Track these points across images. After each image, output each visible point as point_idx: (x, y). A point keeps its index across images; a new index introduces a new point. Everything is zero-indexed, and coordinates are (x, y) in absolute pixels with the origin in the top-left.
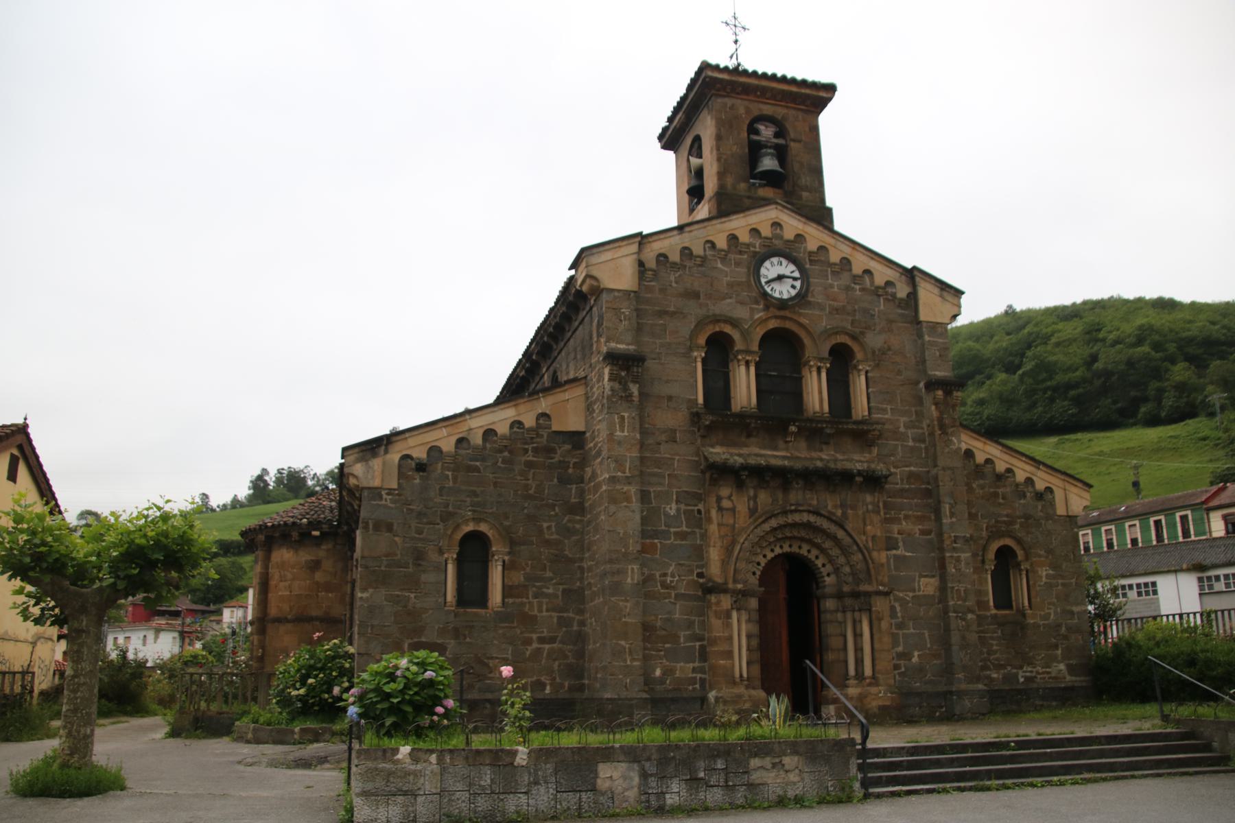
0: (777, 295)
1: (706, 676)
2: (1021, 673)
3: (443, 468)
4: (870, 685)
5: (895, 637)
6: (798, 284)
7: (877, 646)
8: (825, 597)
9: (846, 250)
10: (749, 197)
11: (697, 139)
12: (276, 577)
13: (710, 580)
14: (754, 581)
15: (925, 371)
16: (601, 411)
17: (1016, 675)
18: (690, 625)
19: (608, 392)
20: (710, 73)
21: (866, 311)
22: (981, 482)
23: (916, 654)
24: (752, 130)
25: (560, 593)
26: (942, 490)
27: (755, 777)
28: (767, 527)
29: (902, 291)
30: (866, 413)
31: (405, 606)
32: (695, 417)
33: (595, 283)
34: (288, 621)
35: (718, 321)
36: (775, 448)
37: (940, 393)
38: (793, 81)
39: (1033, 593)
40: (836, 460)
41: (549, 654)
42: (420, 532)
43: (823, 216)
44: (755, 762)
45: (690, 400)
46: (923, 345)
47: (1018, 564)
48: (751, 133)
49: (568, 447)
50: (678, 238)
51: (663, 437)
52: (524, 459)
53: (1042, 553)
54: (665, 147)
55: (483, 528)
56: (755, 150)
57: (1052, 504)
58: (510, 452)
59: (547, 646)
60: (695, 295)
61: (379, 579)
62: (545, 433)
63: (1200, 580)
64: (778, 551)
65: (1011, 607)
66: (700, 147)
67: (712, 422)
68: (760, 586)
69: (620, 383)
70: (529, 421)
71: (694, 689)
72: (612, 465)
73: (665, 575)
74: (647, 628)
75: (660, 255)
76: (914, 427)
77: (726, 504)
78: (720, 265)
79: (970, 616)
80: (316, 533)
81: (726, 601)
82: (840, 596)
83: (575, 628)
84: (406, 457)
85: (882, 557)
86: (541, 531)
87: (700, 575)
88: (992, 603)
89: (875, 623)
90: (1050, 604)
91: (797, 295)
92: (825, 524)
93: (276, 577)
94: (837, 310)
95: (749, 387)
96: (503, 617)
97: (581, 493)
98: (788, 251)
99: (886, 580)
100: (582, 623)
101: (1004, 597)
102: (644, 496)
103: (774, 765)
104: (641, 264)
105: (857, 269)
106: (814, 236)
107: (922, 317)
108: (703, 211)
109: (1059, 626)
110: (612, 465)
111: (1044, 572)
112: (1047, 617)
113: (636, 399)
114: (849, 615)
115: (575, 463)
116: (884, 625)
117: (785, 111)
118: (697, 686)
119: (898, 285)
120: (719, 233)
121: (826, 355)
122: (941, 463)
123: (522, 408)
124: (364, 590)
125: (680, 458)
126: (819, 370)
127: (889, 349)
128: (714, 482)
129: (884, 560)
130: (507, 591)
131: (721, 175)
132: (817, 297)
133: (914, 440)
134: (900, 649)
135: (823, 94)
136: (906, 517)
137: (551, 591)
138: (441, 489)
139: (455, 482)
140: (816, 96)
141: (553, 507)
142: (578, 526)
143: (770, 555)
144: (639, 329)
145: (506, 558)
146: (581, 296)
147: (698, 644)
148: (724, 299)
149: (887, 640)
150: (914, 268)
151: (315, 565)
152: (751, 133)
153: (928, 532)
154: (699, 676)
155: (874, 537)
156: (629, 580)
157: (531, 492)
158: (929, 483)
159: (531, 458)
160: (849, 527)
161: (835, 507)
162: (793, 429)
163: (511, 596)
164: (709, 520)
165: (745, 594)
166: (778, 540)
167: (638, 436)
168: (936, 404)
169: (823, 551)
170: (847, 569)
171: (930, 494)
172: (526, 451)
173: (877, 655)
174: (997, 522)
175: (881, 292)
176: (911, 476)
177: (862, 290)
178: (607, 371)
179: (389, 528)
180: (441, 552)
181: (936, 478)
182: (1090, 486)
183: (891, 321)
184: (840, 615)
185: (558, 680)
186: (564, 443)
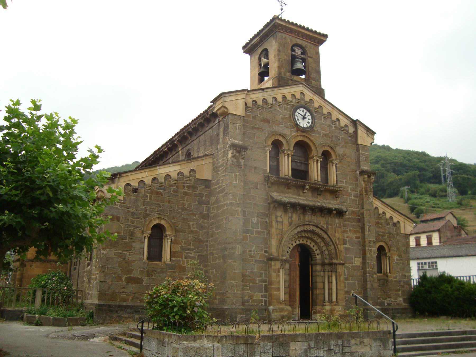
0: (302, 125)
1: (267, 299)
2: (386, 302)
4: (335, 305)
6: (310, 122)
7: (338, 288)
8: (316, 264)
10: (291, 80)
13: (271, 254)
14: (288, 255)
15: (359, 166)
16: (225, 171)
17: (384, 303)
18: (261, 274)
19: (230, 162)
20: (278, 21)
21: (336, 137)
24: (293, 50)
25: (197, 257)
26: (366, 219)
27: (353, 349)
28: (296, 231)
29: (351, 130)
31: (124, 259)
32: (267, 179)
33: (226, 110)
35: (277, 134)
36: (299, 195)
37: (366, 176)
38: (311, 31)
39: (391, 267)
40: (325, 203)
43: (320, 92)
44: (353, 342)
45: (264, 170)
46: (359, 155)
47: (386, 254)
48: (288, 51)
49: (203, 187)
50: (261, 94)
51: (252, 186)
52: (183, 191)
53: (395, 249)
54: (245, 52)
55: (163, 222)
56: (294, 59)
57: (399, 228)
58: (177, 187)
60: (268, 121)
62: (193, 179)
63: (418, 264)
64: (298, 242)
65: (381, 272)
67: (274, 181)
69: (236, 158)
70: (186, 172)
71: (262, 305)
72: (231, 197)
73: (251, 251)
74: (244, 276)
75: (254, 101)
76: (354, 191)
77: (279, 219)
78: (278, 109)
81: (277, 265)
82: (323, 264)
84: (128, 185)
85: (342, 248)
86: (189, 226)
87: (266, 252)
90: (397, 272)
91: (310, 126)
94: (326, 135)
97: (208, 209)
98: (307, 106)
99: (343, 258)
103: (360, 343)
104: (246, 104)
105: (334, 118)
106: (317, 101)
107: (360, 142)
108: (268, 82)
109: (400, 281)
110: (231, 197)
111: (395, 258)
112: (395, 277)
113: (243, 167)
114: (326, 273)
115: (206, 195)
116: (342, 278)
117: (306, 43)
118: (263, 304)
119: (350, 127)
120: (279, 93)
122: (365, 207)
125: (259, 196)
127: (345, 155)
130: (172, 254)
131: (279, 68)
132: (317, 128)
133: (354, 196)
134: (346, 289)
136: (350, 230)
137: (193, 255)
138: (144, 202)
139: (151, 199)
140: (319, 39)
141: (195, 215)
142: (206, 225)
143: (295, 244)
144: (244, 134)
145: (173, 238)
146: (215, 115)
147: (264, 284)
148: (280, 124)
149: (342, 285)
150: (357, 120)
152: (288, 51)
154: (264, 299)
155: (339, 239)
156: (237, 253)
157: (186, 207)
158: (359, 216)
159: (186, 191)
160: (329, 233)
161: (324, 223)
163: (175, 257)
164: (271, 226)
165: (286, 261)
167: (243, 184)
168: (364, 181)
170: (326, 253)
171: (360, 220)
172: (184, 187)
173: (339, 292)
174: (378, 235)
177: (336, 127)
179: (118, 219)
180: (143, 233)
181: (363, 214)
184: (322, 273)
186: (201, 184)
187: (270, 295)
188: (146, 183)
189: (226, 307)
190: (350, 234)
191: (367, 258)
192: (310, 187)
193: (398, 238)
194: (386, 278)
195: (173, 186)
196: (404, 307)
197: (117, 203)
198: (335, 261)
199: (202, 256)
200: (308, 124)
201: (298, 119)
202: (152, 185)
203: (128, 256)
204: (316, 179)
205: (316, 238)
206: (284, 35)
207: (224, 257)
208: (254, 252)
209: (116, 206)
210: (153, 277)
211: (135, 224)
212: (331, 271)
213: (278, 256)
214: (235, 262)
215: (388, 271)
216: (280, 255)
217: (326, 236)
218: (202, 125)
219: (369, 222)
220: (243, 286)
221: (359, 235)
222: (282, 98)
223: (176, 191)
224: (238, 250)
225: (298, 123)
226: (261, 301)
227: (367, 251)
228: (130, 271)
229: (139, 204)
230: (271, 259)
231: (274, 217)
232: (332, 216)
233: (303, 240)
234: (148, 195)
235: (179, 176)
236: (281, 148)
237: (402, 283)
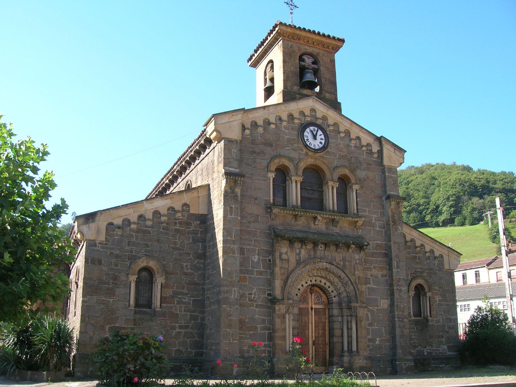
0: (312, 147)
6: (323, 142)
7: (359, 335)
9: (347, 125)
10: (299, 94)
11: (271, 62)
15: (385, 192)
17: (423, 351)
18: (264, 321)
21: (357, 158)
23: (378, 339)
24: (301, 59)
26: (393, 254)
29: (375, 148)
30: (356, 212)
42: (116, 265)
43: (336, 106)
45: (266, 200)
46: (385, 178)
49: (199, 222)
53: (437, 288)
56: (302, 70)
58: (167, 224)
65: (421, 316)
70: (178, 206)
73: (251, 294)
74: (241, 322)
77: (284, 257)
79: (405, 320)
83: (199, 321)
85: (363, 288)
86: (182, 268)
88: (412, 314)
89: (359, 322)
91: (323, 147)
92: (336, 270)
94: (343, 157)
99: (364, 300)
100: (203, 319)
102: (242, 251)
109: (444, 326)
111: (437, 298)
112: (438, 322)
116: (363, 324)
119: (373, 145)
129: (363, 290)
130: (163, 300)
133: (379, 227)
134: (370, 337)
135: (339, 44)
136: (375, 268)
137: (186, 300)
139: (136, 239)
153: (386, 276)
154: (267, 349)
155: (359, 278)
156: (232, 297)
159: (178, 228)
160: (347, 271)
163: (165, 303)
164: (275, 265)
167: (239, 218)
171: (388, 255)
172: (176, 223)
173: (359, 340)
174: (416, 271)
176: (377, 245)
179: (100, 262)
181: (390, 247)
185: (189, 349)
187: (274, 345)
190: (374, 272)
191: (396, 301)
197: (98, 245)
200: (320, 145)
201: (308, 140)
204: (331, 208)
205: (331, 277)
207: (218, 302)
209: (97, 248)
211: (119, 267)
212: (351, 316)
214: (231, 308)
215: (429, 314)
217: (343, 275)
218: (198, 153)
219: (397, 256)
220: (240, 334)
221: (385, 272)
224: (234, 294)
225: (308, 144)
234: (134, 234)
235: (170, 211)
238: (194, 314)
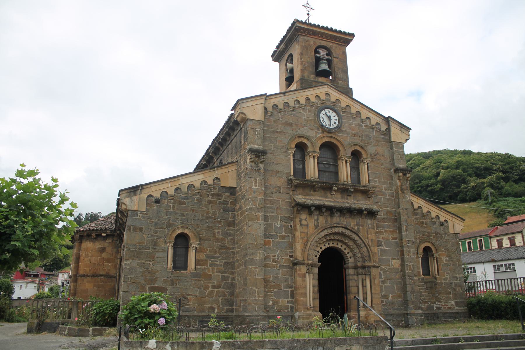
1: (293, 305)
2: (435, 306)
3: (168, 202)
5: (381, 287)
6: (337, 122)
7: (373, 292)
8: (348, 268)
9: (359, 108)
10: (315, 82)
11: (291, 55)
12: (84, 255)
13: (296, 259)
14: (316, 260)
16: (245, 177)
17: (433, 307)
18: (286, 280)
19: (249, 167)
20: (298, 24)
21: (367, 136)
22: (416, 217)
23: (391, 295)
24: (316, 52)
25: (223, 264)
28: (323, 234)
29: (384, 127)
31: (147, 269)
33: (244, 116)
34: (88, 276)
35: (301, 137)
36: (327, 197)
37: (401, 174)
38: (335, 31)
39: (439, 268)
40: (355, 203)
41: (217, 294)
43: (348, 92)
45: (287, 173)
46: (393, 152)
47: (433, 255)
48: (315, 53)
49: (229, 194)
51: (275, 190)
55: (186, 231)
56: (318, 61)
57: (447, 227)
59: (216, 290)
60: (291, 125)
61: (136, 255)
63: (494, 266)
65: (429, 275)
66: (292, 59)
67: (298, 184)
68: (319, 262)
69: (255, 163)
70: (210, 181)
71: (288, 311)
72: (251, 202)
73: (274, 256)
74: (266, 281)
75: (274, 105)
77: (304, 222)
78: (301, 111)
79: (415, 278)
80: (104, 235)
81: (303, 269)
82: (356, 268)
83: (230, 281)
84: (151, 196)
85: (375, 249)
86: (214, 234)
87: (291, 256)
88: (421, 273)
89: (372, 280)
90: (447, 273)
93: (84, 255)
94: (354, 135)
95: (314, 168)
96: (196, 275)
97: (234, 216)
100: (233, 279)
101: (427, 271)
102: (266, 218)
104: (266, 109)
105: (363, 117)
106: (344, 101)
107: (393, 139)
108: (293, 87)
109: (451, 283)
111: (444, 259)
112: (446, 279)
114: (360, 277)
115: (231, 202)
116: (376, 281)
117: (331, 44)
118: (289, 310)
120: (302, 96)
121: (350, 155)
122: (402, 206)
123: (207, 175)
124: (128, 260)
125: (282, 200)
126: (346, 161)
127: (378, 154)
128: (298, 212)
129: (376, 251)
130: (198, 262)
131: (302, 71)
132: (345, 128)
134: (383, 293)
136: (386, 231)
137: (218, 263)
138: (167, 212)
139: (173, 209)
140: (345, 38)
141: (220, 222)
142: (232, 232)
143: (324, 248)
144: (264, 138)
145: (197, 246)
146: (236, 123)
147: (290, 289)
148: (304, 127)
149: (378, 289)
150: (389, 117)
151: (103, 250)
152: (315, 53)
153: (396, 239)
154: (290, 305)
155: (371, 240)
156: (258, 258)
158: (395, 216)
159: (210, 199)
161: (354, 225)
162: (335, 188)
163: (200, 265)
164: (296, 230)
165: (312, 265)
166: (328, 240)
167: (263, 189)
168: (399, 179)
169: (348, 246)
170: (359, 255)
171: (397, 220)
172: (208, 195)
173: (373, 296)
174: (423, 235)
175: (374, 127)
176: (388, 212)
177: (366, 126)
178: (249, 158)
179: (141, 230)
180: (166, 243)
181: (399, 213)
182: (464, 220)
183: (378, 141)
184: (355, 277)
185: (221, 306)
186: (226, 192)
187: (296, 301)
188: (169, 193)
189: (247, 314)
190: (385, 235)
191: (406, 260)
192: (338, 188)
193: (446, 237)
194: (434, 280)
195: (196, 195)
196: (457, 311)
197: (139, 215)
198: (367, 264)
199: (228, 263)
200: (334, 124)
201: (323, 120)
202: (174, 196)
203: (151, 266)
204: (346, 180)
206: (306, 38)
207: (245, 263)
208: (278, 256)
209: (139, 217)
210: (178, 286)
211: (158, 234)
212: (365, 274)
213: (304, 260)
214: (256, 268)
215: (437, 273)
216: (306, 259)
217: (357, 238)
218: (228, 134)
220: (265, 292)
222: (306, 100)
223: (199, 200)
225: (324, 124)
226: (287, 307)
227: (405, 252)
228: (154, 281)
229: (162, 215)
230: (295, 264)
231: (298, 221)
232: (363, 217)
233: (333, 244)
234: (171, 205)
235: (203, 185)
236: (306, 150)
237: (453, 286)
238: (225, 275)
